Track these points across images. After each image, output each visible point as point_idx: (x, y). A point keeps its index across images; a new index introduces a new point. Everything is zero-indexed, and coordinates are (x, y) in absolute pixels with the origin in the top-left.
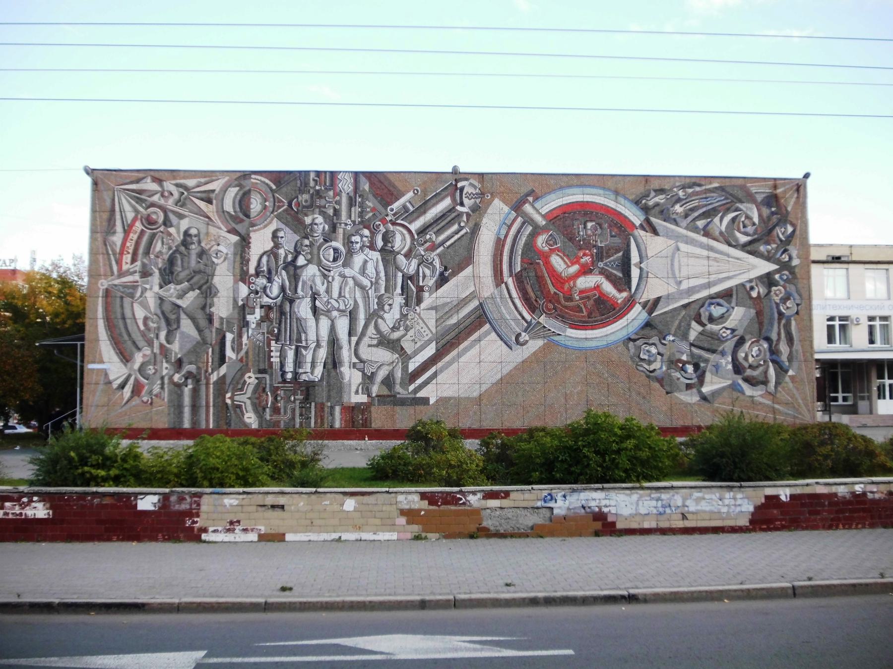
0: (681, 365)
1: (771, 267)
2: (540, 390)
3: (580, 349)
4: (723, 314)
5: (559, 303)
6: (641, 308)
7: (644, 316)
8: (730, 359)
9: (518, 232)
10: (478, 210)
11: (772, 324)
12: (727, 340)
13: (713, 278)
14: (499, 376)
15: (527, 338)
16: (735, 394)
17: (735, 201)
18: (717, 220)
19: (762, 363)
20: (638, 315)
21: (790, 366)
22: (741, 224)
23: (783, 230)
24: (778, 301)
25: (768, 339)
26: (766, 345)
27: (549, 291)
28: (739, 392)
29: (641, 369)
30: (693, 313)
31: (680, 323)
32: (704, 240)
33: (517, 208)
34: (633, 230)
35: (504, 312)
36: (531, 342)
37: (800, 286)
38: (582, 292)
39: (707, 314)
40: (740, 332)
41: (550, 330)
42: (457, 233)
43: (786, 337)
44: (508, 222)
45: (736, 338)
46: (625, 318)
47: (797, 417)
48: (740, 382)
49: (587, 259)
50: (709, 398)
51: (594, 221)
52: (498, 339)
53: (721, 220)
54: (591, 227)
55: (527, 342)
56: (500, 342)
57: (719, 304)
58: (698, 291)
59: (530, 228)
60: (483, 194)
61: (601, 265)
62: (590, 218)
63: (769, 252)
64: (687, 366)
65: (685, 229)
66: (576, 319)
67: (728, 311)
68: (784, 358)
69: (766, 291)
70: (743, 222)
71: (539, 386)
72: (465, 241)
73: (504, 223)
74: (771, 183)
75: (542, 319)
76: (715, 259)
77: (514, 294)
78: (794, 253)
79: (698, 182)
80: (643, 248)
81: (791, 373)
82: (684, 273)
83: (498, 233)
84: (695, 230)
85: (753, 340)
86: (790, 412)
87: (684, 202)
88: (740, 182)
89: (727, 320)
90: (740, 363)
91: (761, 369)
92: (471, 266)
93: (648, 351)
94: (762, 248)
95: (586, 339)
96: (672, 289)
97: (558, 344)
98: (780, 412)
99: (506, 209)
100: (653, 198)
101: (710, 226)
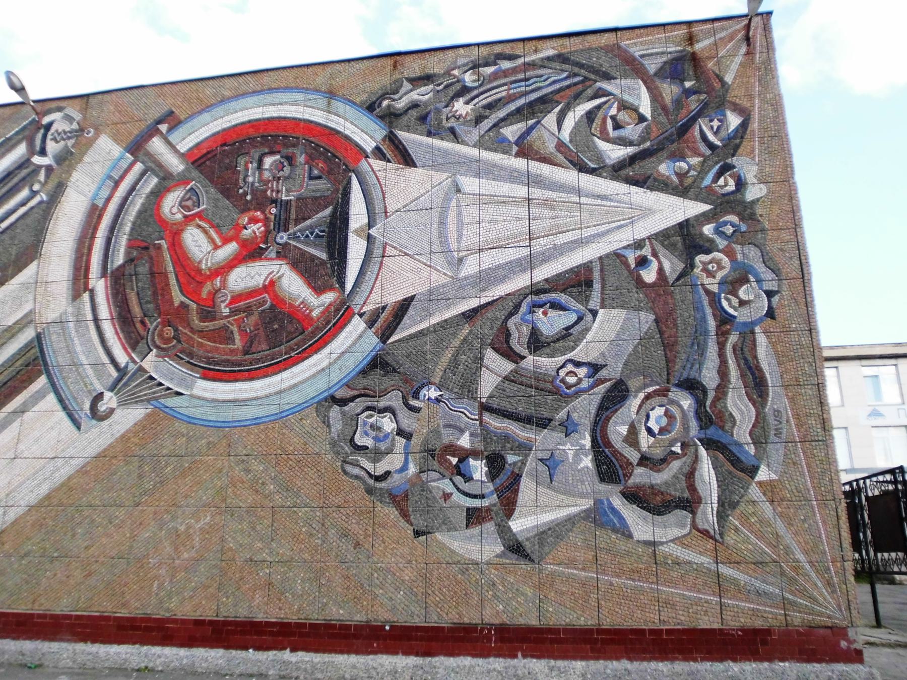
0: (454, 461)
1: (694, 208)
2: (122, 521)
3: (218, 426)
4: (567, 329)
5: (189, 325)
6: (363, 326)
7: (371, 342)
8: (587, 442)
9: (132, 189)
10: (66, 159)
11: (702, 352)
12: (577, 394)
13: (539, 245)
14: (44, 489)
15: (114, 404)
16: (606, 537)
17: (593, 77)
18: (550, 120)
19: (677, 449)
20: (354, 343)
21: (758, 457)
22: (609, 121)
23: (716, 124)
24: (715, 288)
25: (692, 386)
26: (687, 402)
27: (171, 302)
28: (615, 530)
29: (356, 471)
30: (489, 331)
31: (455, 356)
32: (520, 164)
33: (137, 148)
34: (359, 161)
35: (79, 349)
36: (118, 413)
37: (773, 248)
38: (237, 298)
39: (526, 330)
40: (614, 370)
41: (160, 384)
42: (23, 204)
43: (743, 376)
44: (116, 176)
45: (602, 389)
46: (326, 351)
47: (793, 603)
48: (618, 502)
49: (255, 230)
50: (527, 545)
51: (279, 152)
52: (58, 407)
53: (560, 122)
54: (272, 165)
55: (112, 411)
56: (62, 414)
57: (557, 306)
58: (503, 279)
59: (154, 181)
60: (81, 130)
61: (283, 237)
62: (270, 147)
63: (681, 176)
64: (472, 462)
65: (474, 146)
66: (217, 357)
67: (580, 319)
68: (742, 433)
69: (680, 266)
70: (613, 118)
71: (121, 513)
72: (36, 215)
73: (110, 177)
74: (682, 31)
75: (150, 362)
76: (546, 203)
77: (104, 312)
78: (750, 172)
79: (507, 49)
80: (376, 194)
81: (763, 474)
82: (470, 237)
83: (96, 195)
84: (500, 145)
85: (651, 389)
86: (770, 589)
87: (475, 92)
88: (605, 39)
89: (577, 342)
90: (616, 453)
91: (676, 465)
92: (35, 263)
93: (376, 428)
94: (665, 169)
95: (235, 401)
96: (438, 279)
97: (173, 415)
98: (741, 591)
99: (117, 150)
100: (405, 94)
101: (534, 134)
